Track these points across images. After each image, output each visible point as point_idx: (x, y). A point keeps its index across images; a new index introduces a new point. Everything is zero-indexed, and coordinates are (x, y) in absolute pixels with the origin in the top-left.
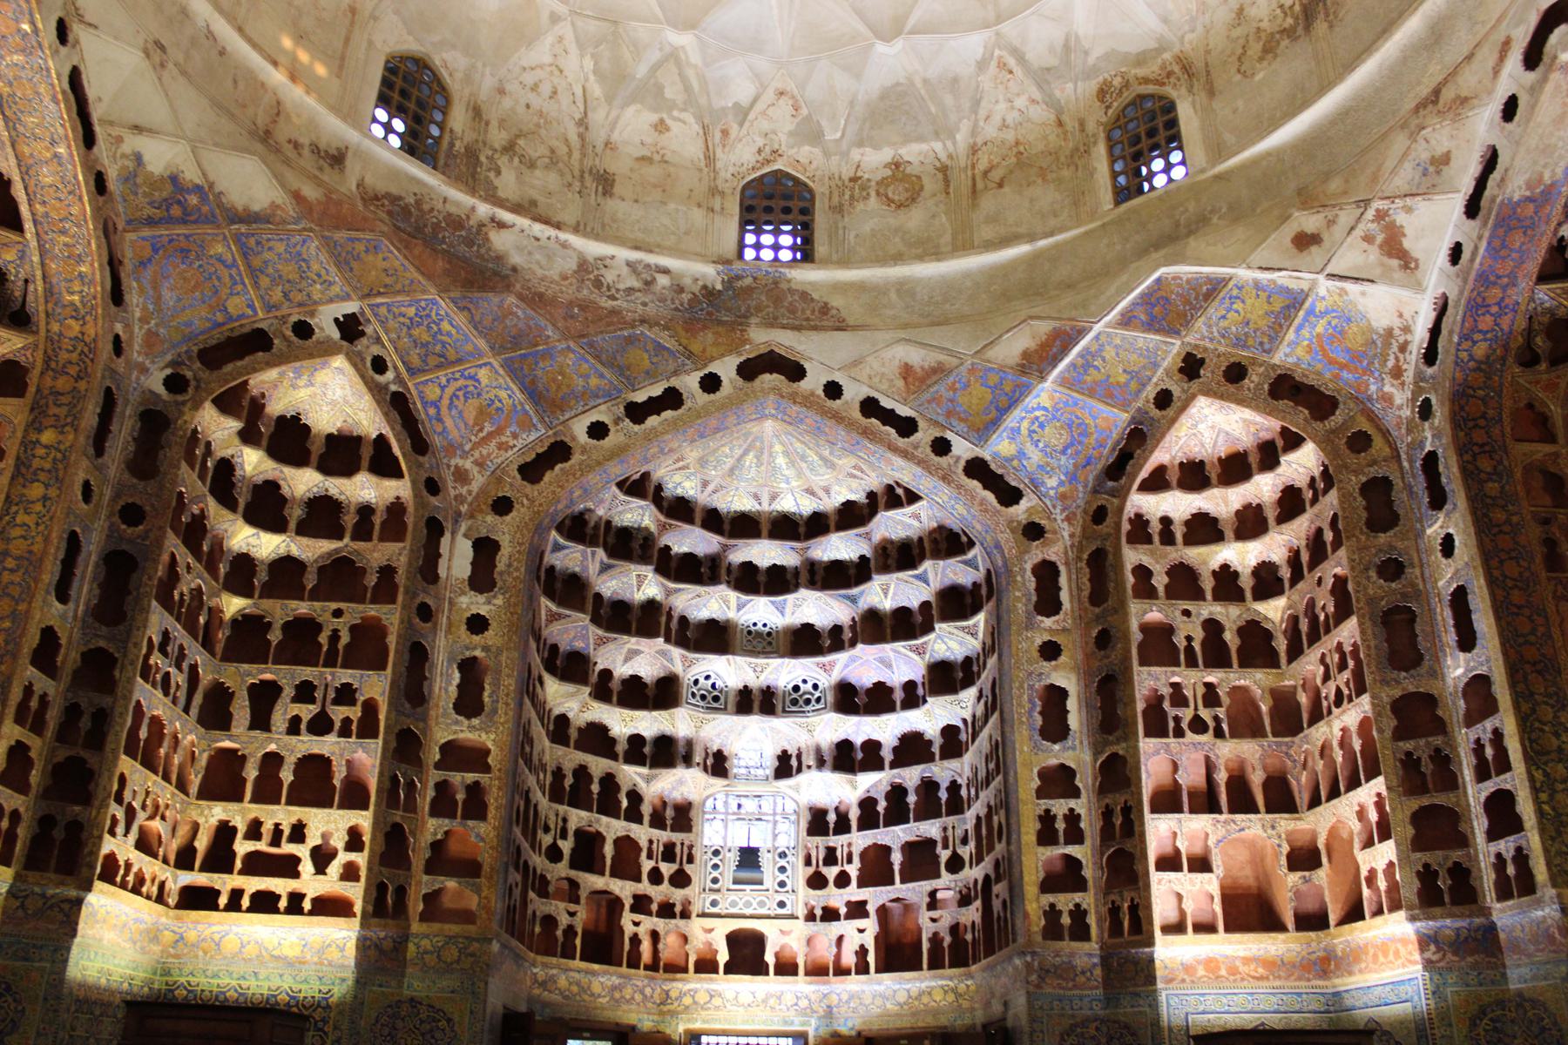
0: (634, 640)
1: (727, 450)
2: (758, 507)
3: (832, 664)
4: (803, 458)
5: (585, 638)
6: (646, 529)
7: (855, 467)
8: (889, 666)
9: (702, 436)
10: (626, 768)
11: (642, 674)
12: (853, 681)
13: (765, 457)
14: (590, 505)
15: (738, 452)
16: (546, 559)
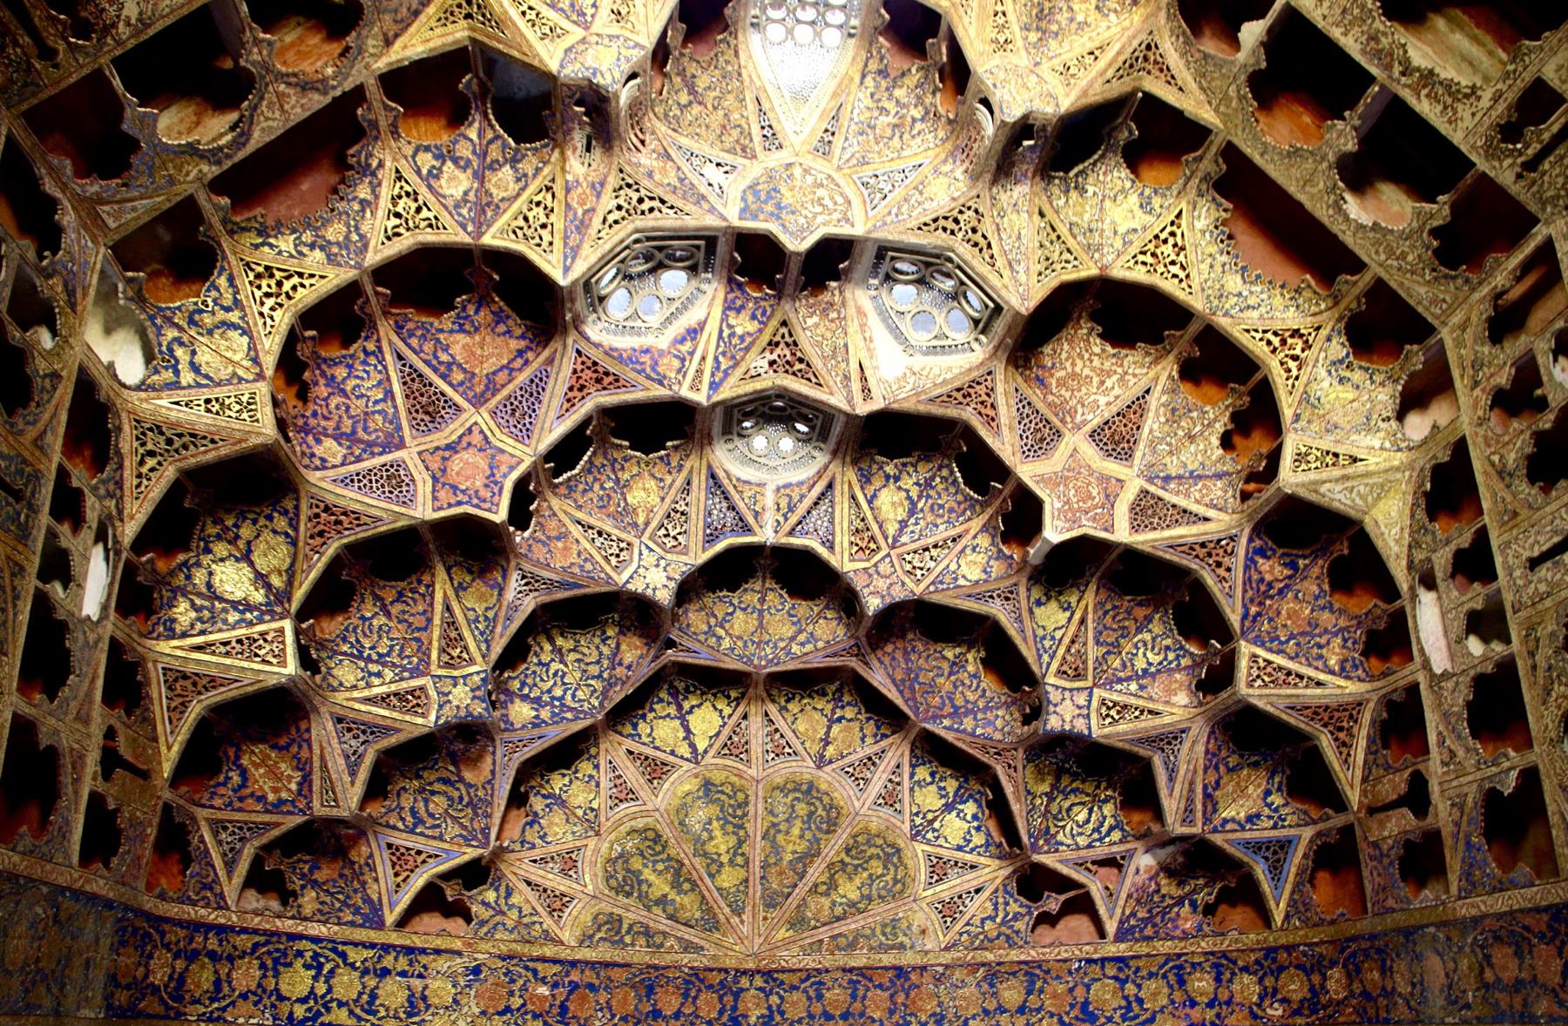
0: (1122, 533)
1: (849, 890)
2: (773, 709)
3: (578, 389)
4: (679, 875)
5: (1260, 592)
6: (1040, 775)
7: (558, 903)
8: (413, 377)
9: (900, 972)
10: (1206, 115)
11: (1097, 345)
12: (517, 325)
13: (757, 850)
14: (1168, 887)
15: (816, 872)
16: (1308, 833)
